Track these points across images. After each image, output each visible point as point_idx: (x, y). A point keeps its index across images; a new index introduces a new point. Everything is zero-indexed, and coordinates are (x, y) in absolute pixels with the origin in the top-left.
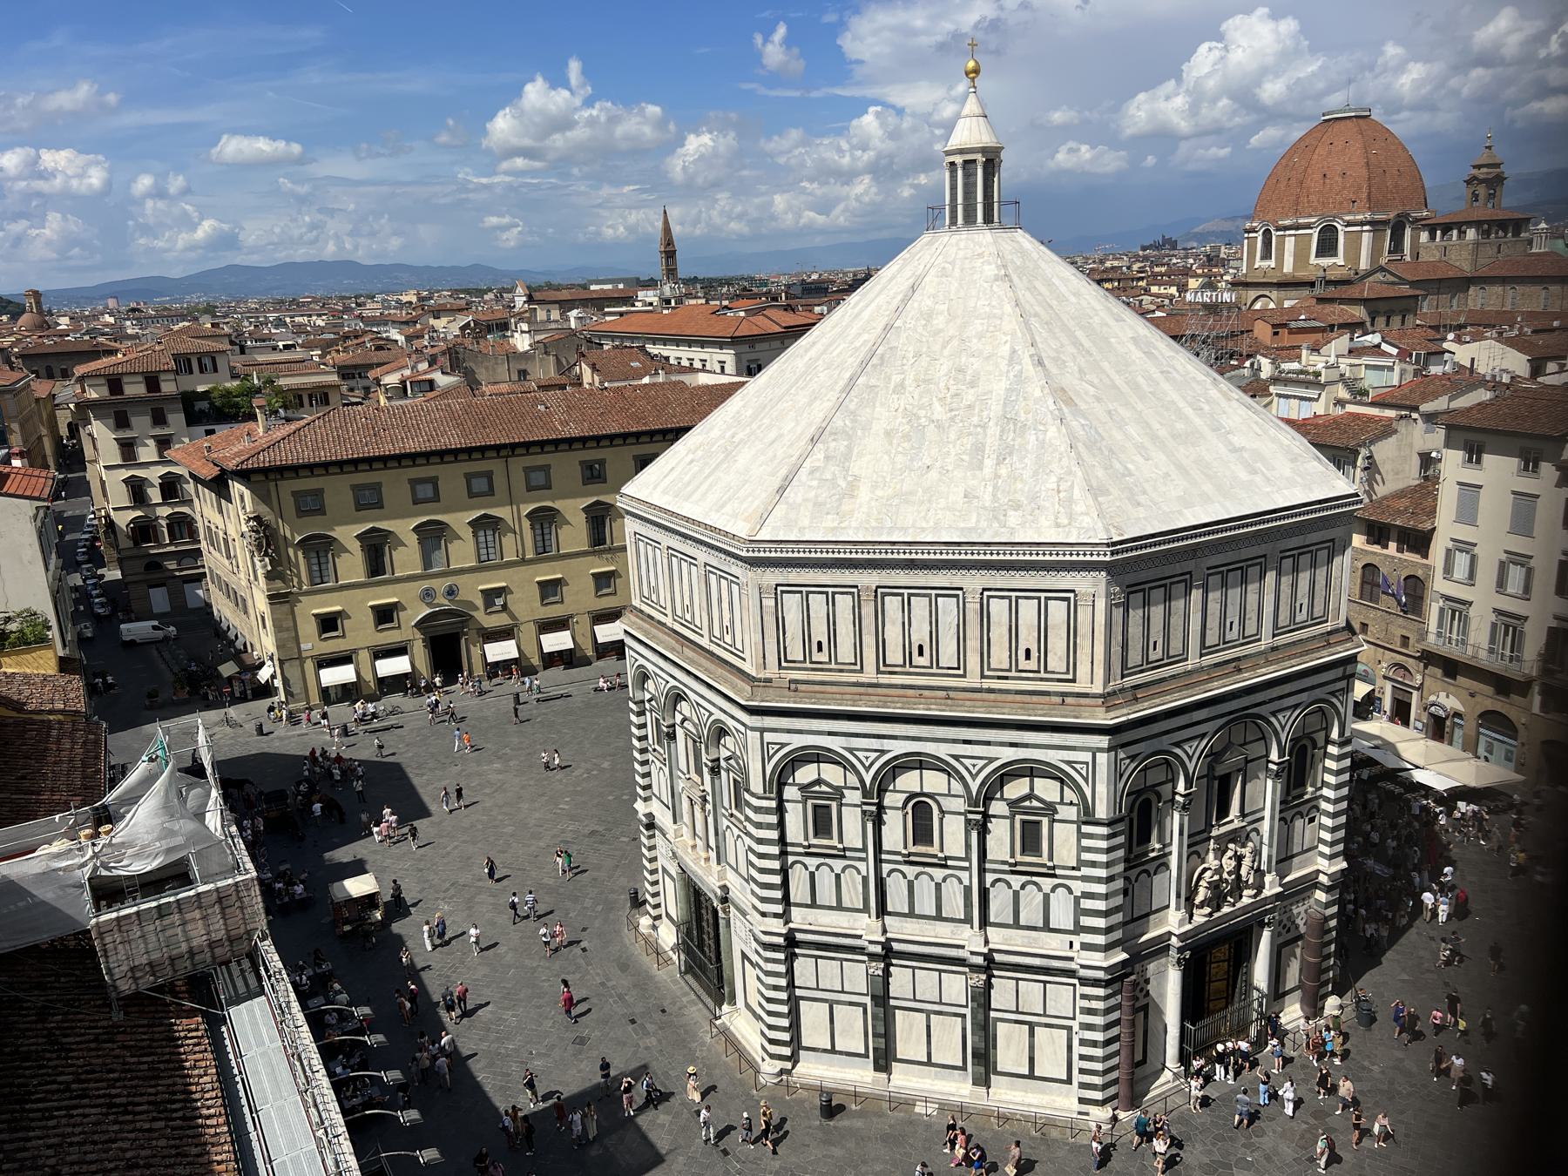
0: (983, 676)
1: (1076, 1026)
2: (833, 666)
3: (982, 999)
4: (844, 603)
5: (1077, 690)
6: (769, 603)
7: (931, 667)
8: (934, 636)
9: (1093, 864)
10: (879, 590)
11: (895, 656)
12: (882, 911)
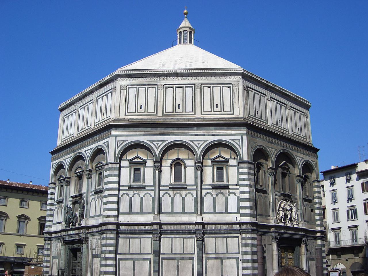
0: (201, 114)
1: (240, 258)
2: (146, 113)
3: (201, 248)
4: (152, 91)
5: (234, 117)
6: (123, 92)
7: (183, 112)
8: (184, 100)
9: (244, 179)
10: (165, 86)
11: (169, 109)
12: (160, 212)
